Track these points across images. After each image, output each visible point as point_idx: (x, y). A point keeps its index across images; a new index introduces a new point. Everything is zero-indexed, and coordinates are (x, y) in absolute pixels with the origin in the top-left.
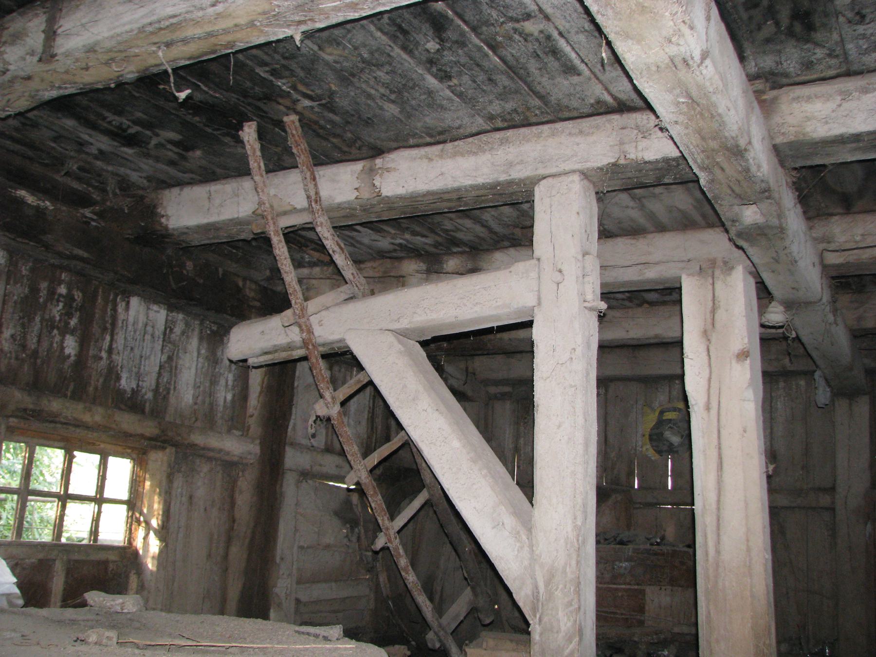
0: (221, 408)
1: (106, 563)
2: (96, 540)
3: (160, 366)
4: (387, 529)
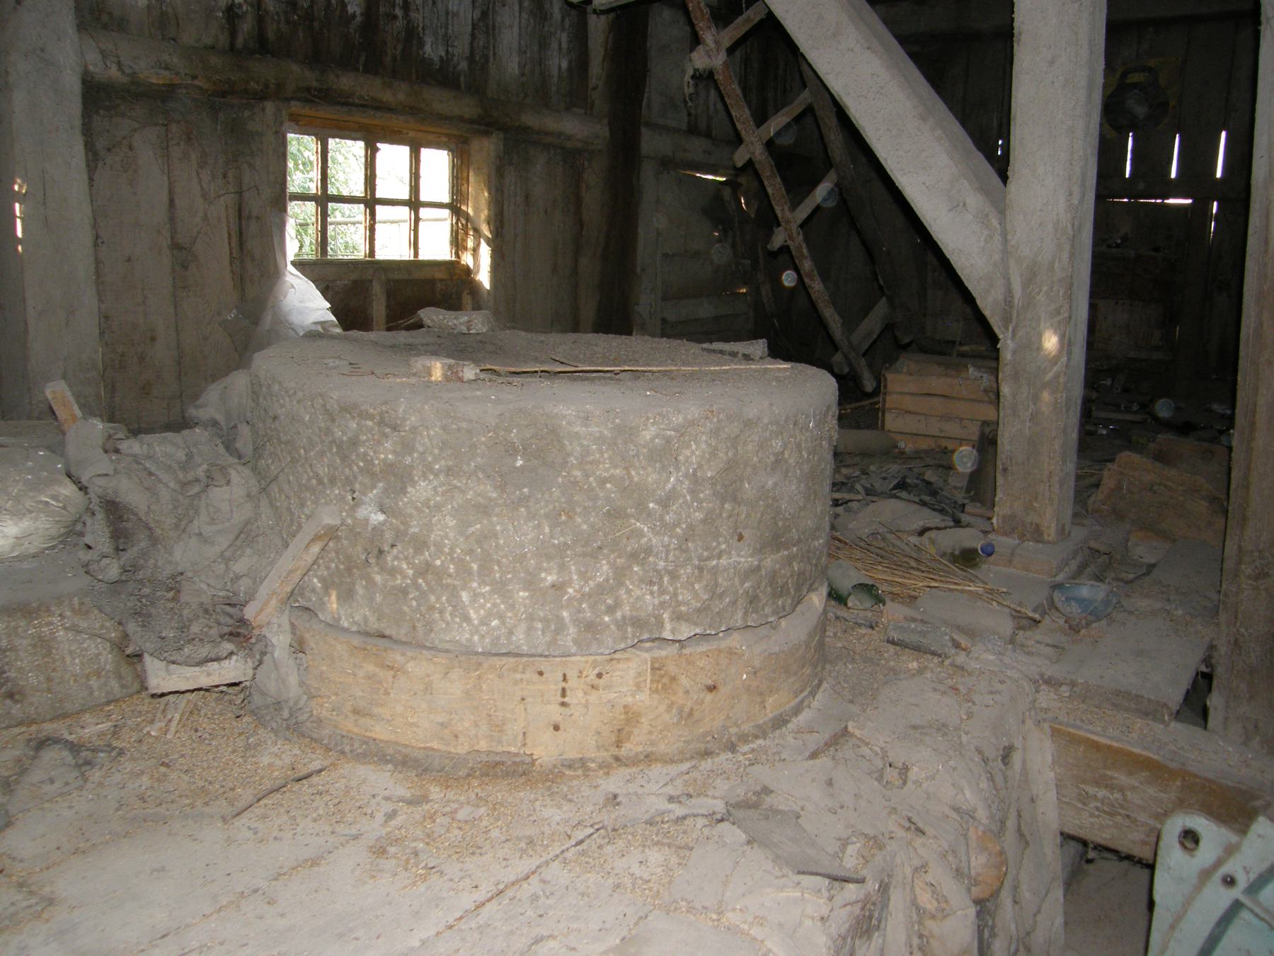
0: (555, 79)
1: (432, 282)
2: (416, 254)
3: (473, 25)
4: (788, 222)
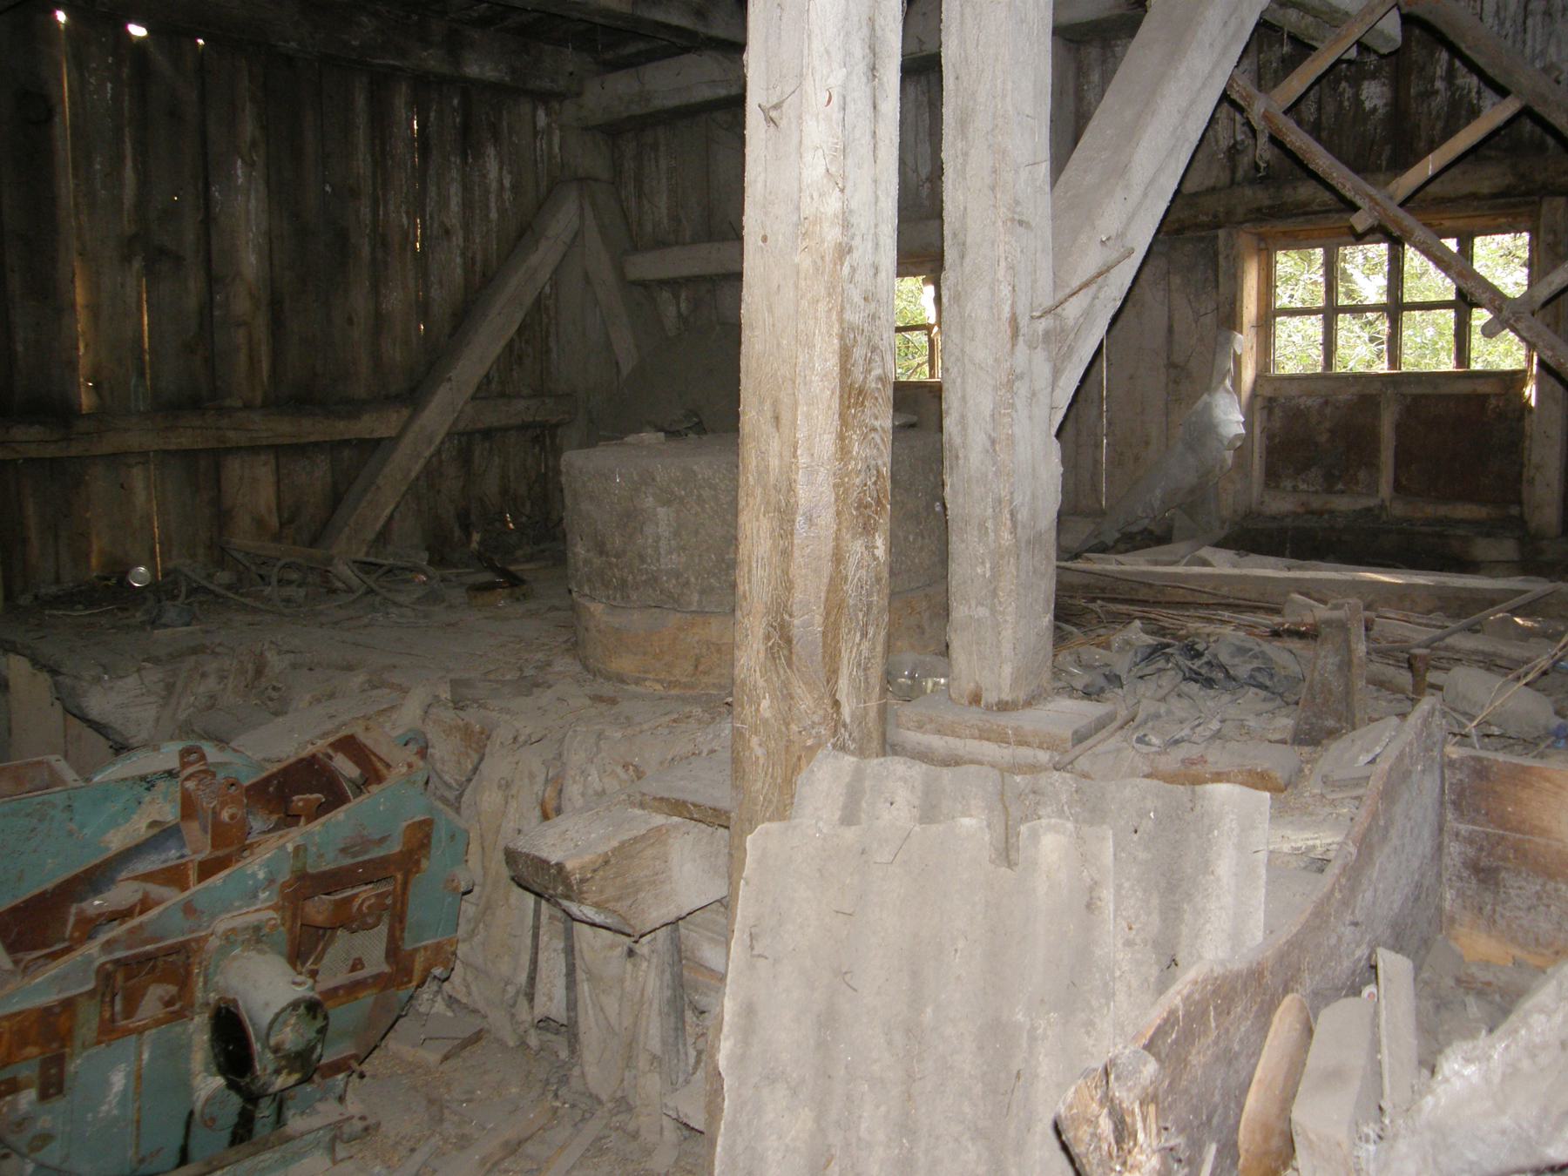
1: (1484, 398)
